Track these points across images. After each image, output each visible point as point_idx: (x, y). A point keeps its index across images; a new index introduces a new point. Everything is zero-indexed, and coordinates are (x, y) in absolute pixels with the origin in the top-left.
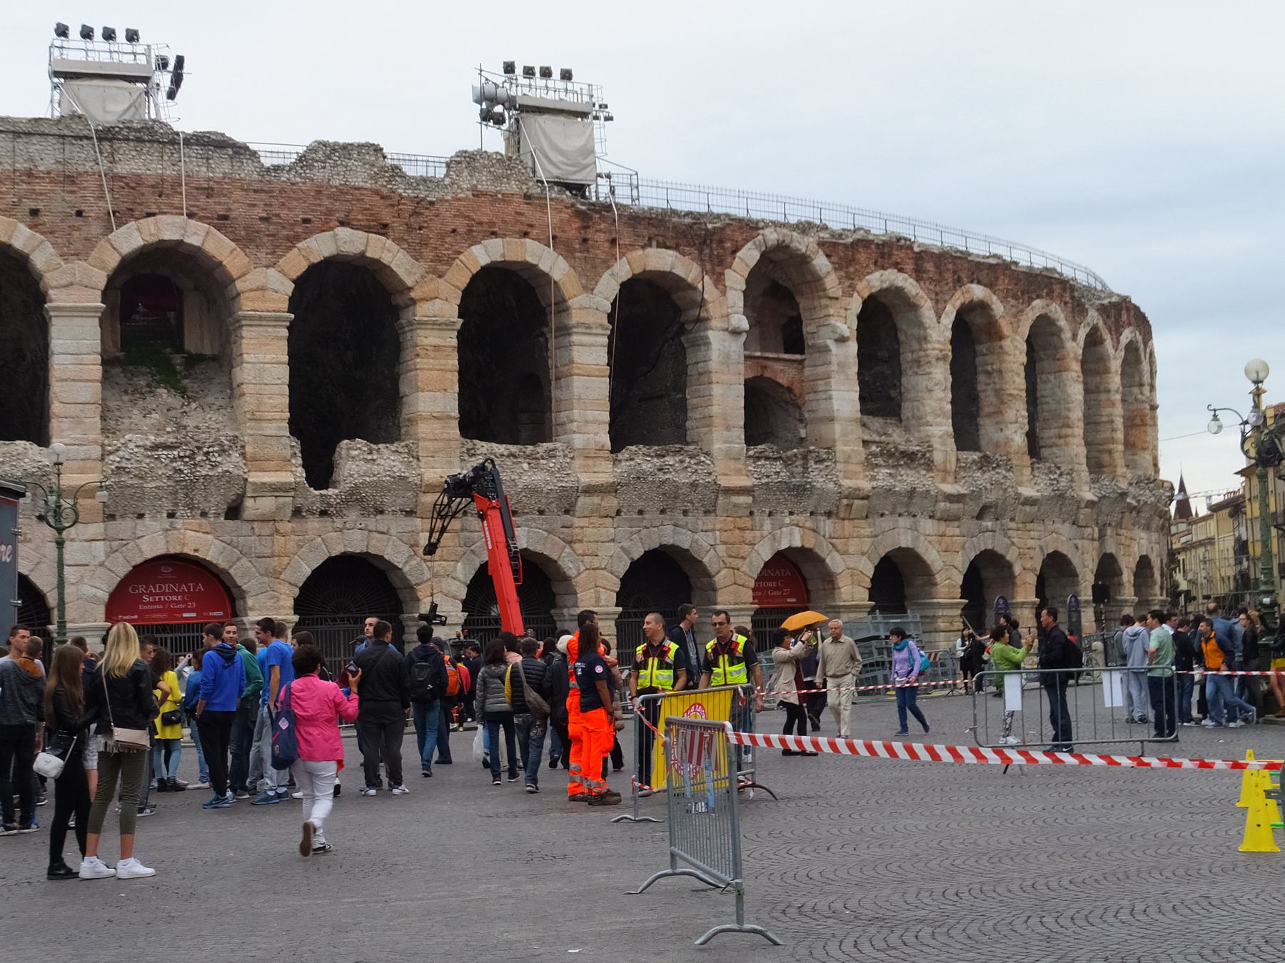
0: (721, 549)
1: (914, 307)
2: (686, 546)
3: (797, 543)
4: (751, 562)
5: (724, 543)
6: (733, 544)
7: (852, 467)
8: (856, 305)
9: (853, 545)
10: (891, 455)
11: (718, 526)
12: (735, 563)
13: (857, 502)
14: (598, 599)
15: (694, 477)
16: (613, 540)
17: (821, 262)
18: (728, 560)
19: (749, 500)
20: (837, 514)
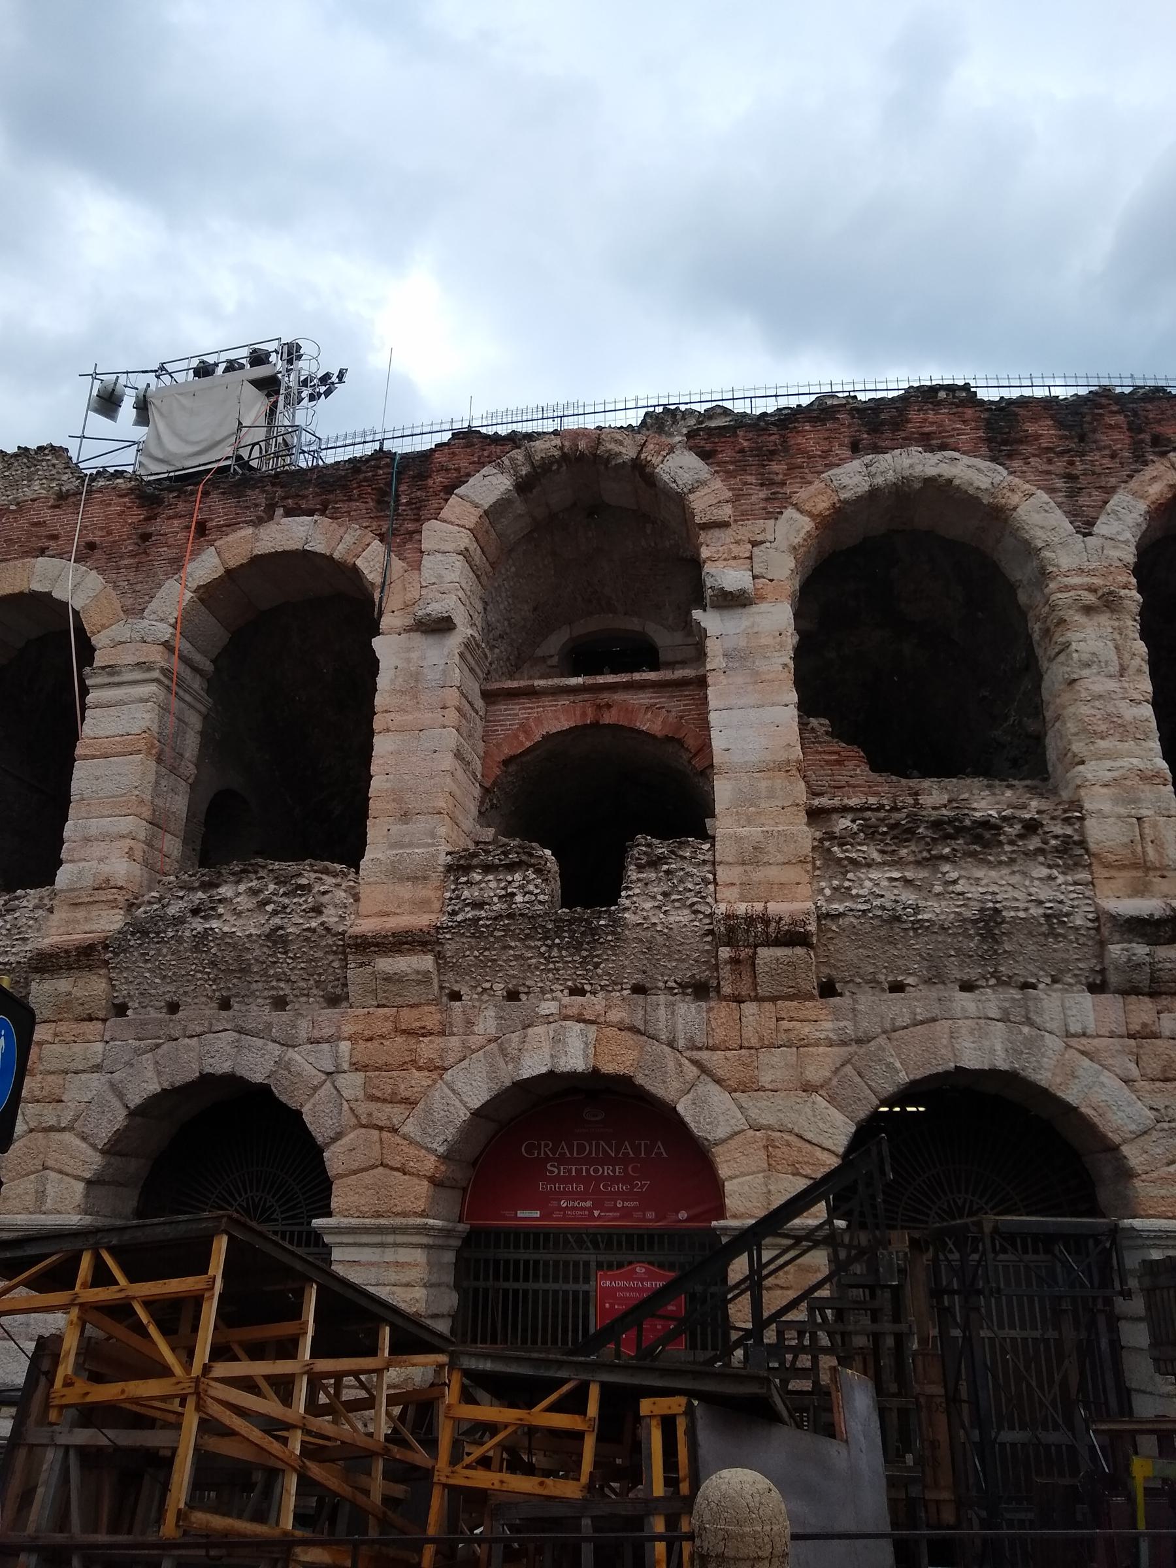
0: (352, 1084)
1: (997, 516)
2: (258, 1078)
3: (574, 1060)
4: (429, 1111)
5: (357, 1067)
6: (386, 1068)
7: (773, 873)
8: (792, 529)
9: (774, 1067)
10: (904, 833)
11: (348, 1029)
12: (384, 1113)
13: (763, 952)
14: (41, 1195)
15: (276, 921)
16: (96, 1068)
17: (680, 467)
18: (363, 1108)
19: (426, 962)
20: (718, 988)
